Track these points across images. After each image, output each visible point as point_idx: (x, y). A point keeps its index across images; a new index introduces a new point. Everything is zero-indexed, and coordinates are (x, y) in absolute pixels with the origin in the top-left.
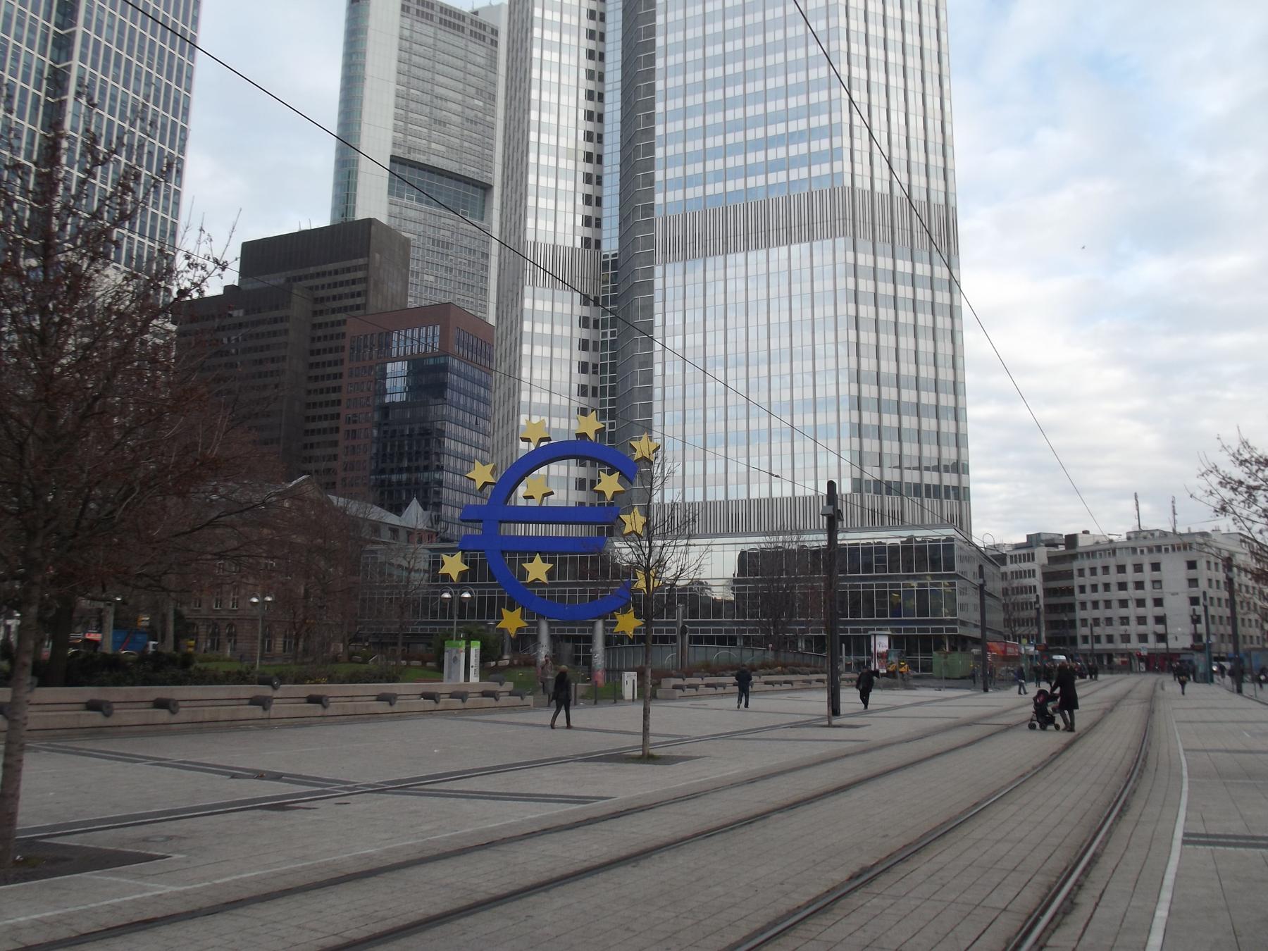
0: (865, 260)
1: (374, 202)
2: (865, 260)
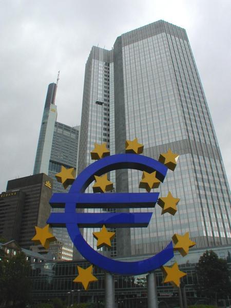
0: (196, 160)
1: (45, 169)
2: (196, 160)
